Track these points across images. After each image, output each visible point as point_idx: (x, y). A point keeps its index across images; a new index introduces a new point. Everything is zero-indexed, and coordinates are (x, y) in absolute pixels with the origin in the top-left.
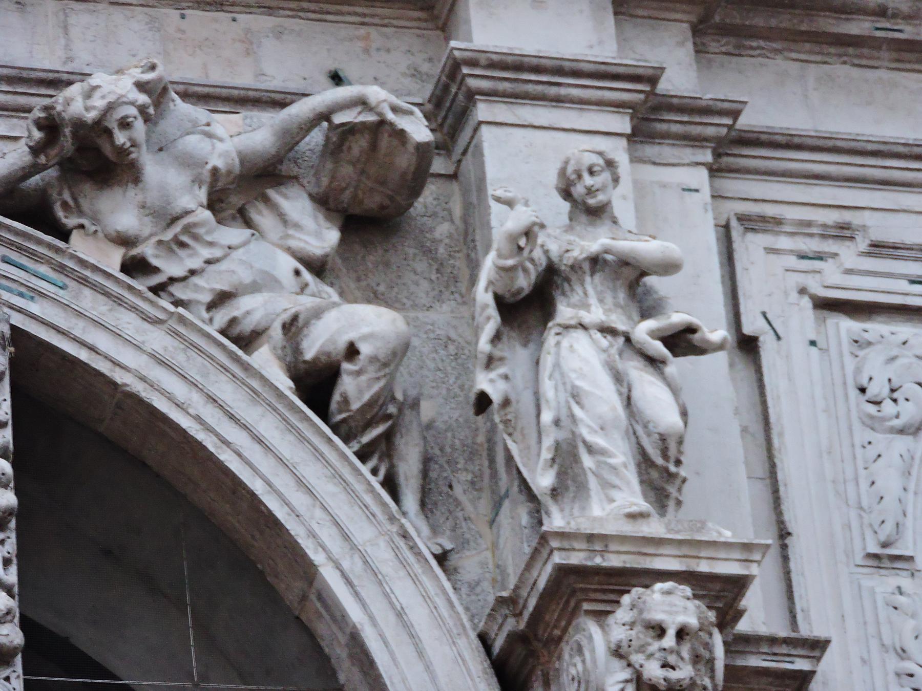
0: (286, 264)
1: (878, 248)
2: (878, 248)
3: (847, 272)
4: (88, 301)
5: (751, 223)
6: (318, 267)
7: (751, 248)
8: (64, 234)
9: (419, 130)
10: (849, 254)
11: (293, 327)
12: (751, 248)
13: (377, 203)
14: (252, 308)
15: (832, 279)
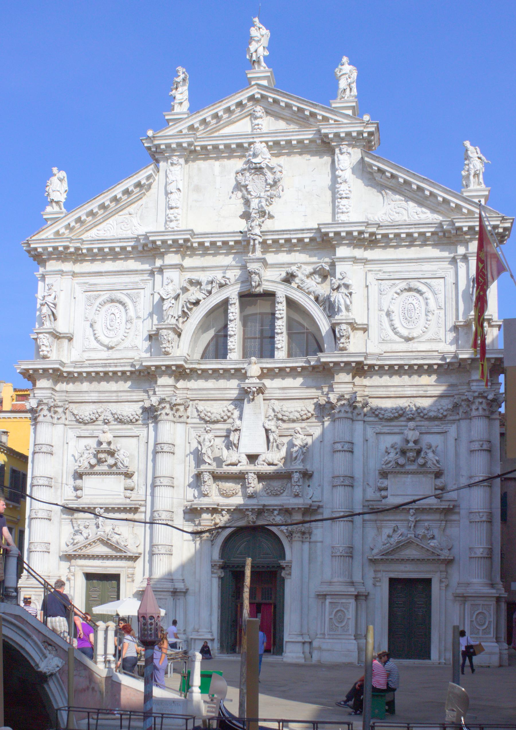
0: (314, 283)
1: (384, 272)
2: (384, 272)
3: (381, 276)
4: (293, 291)
5: (369, 271)
6: (318, 283)
7: (369, 275)
8: (291, 284)
9: (327, 268)
10: (380, 273)
11: (314, 292)
12: (369, 275)
13: (325, 275)
14: (310, 289)
15: (379, 277)
